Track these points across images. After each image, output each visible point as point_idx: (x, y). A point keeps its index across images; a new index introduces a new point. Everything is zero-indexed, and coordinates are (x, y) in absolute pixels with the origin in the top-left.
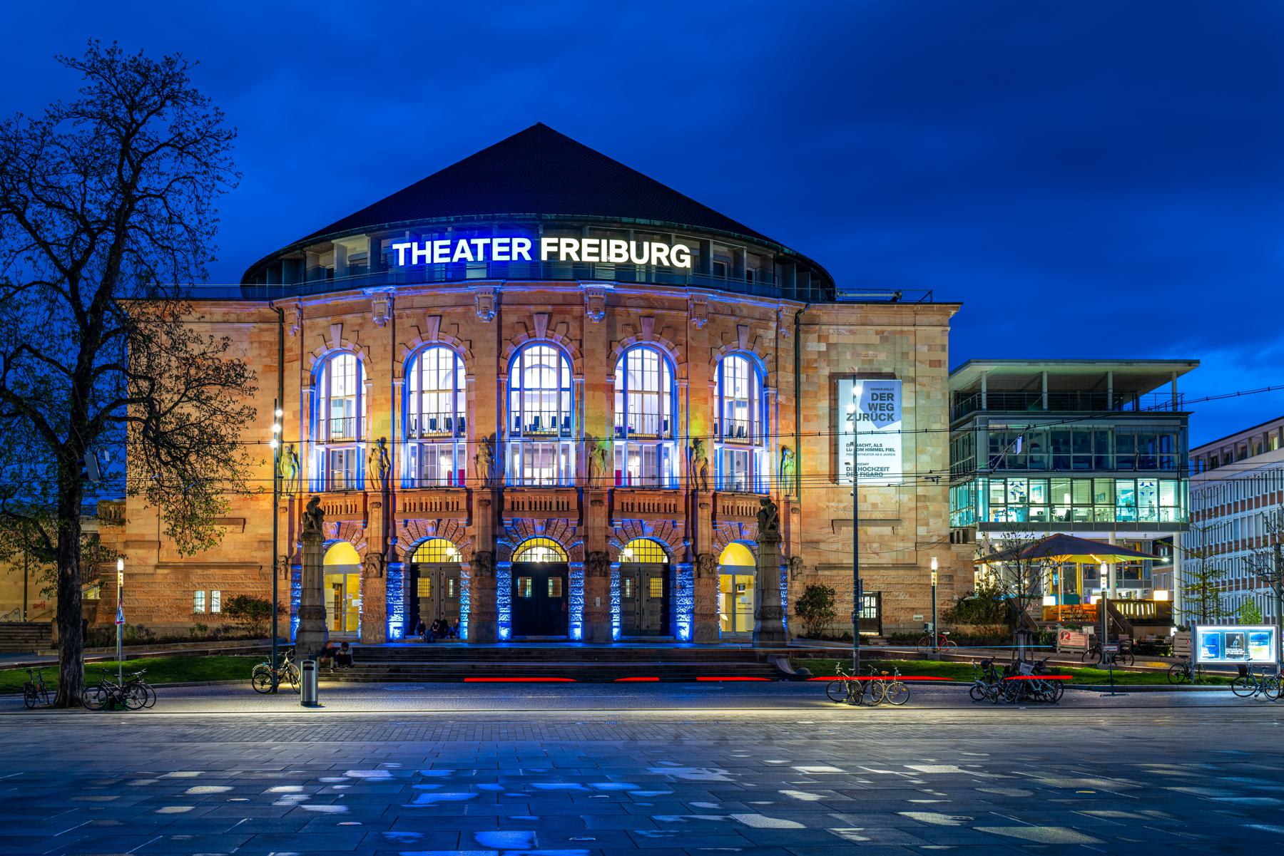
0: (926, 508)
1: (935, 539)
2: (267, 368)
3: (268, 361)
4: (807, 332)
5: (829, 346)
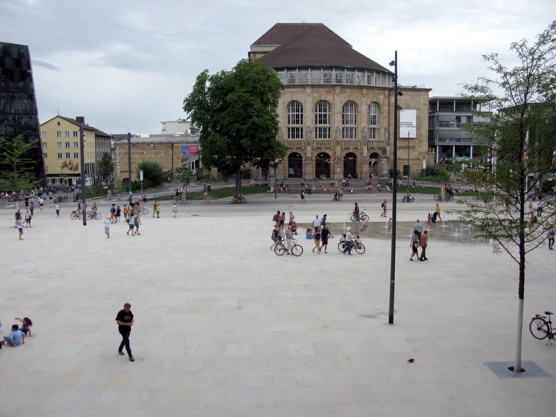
0: (422, 143)
1: (424, 152)
4: (392, 96)
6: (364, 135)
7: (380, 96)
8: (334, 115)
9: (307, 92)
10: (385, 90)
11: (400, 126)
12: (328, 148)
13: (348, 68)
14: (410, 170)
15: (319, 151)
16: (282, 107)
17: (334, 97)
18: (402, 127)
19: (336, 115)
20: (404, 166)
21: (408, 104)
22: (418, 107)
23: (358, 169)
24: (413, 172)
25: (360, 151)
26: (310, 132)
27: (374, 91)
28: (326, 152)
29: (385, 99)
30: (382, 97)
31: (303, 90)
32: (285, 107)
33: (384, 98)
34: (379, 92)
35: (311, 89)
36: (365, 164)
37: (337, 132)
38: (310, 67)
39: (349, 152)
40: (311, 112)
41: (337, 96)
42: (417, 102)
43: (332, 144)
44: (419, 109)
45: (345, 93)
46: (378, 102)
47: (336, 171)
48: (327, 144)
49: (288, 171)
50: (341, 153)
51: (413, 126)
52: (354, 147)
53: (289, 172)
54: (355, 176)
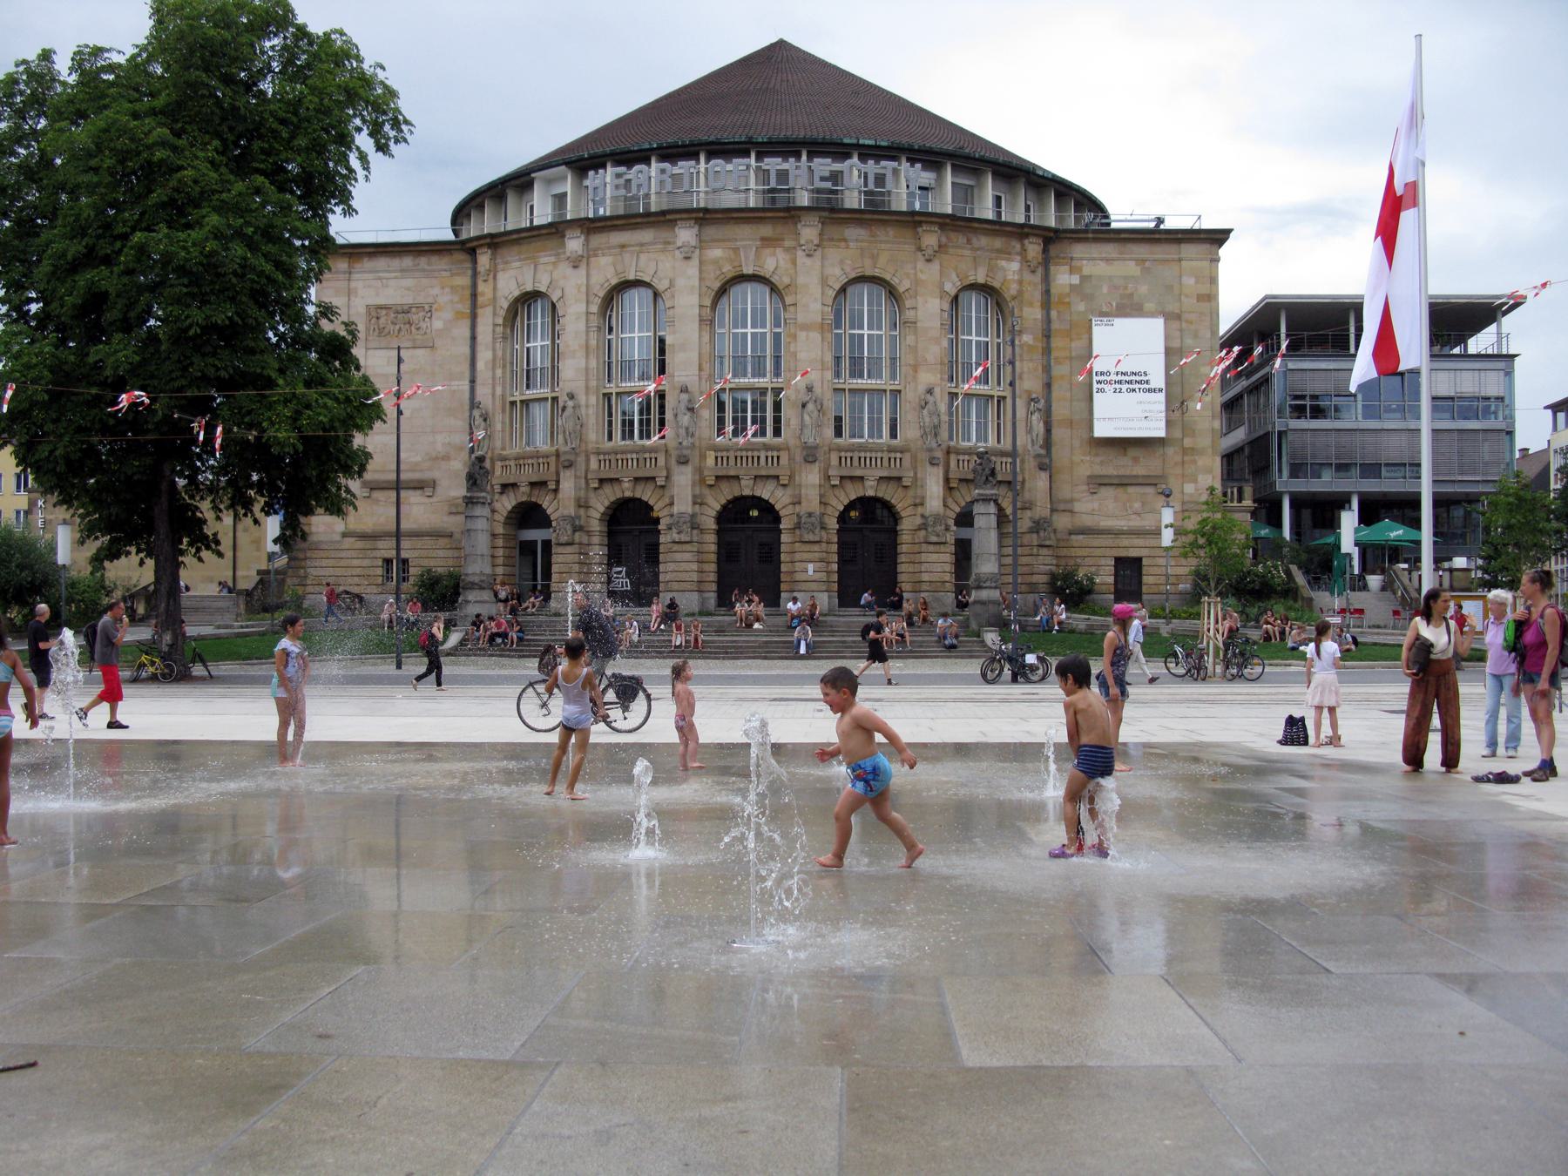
0: (1194, 462)
2: (459, 315)
3: (460, 307)
5: (1084, 279)
6: (927, 420)
7: (1003, 263)
8: (795, 336)
9: (679, 244)
10: (1027, 236)
11: (1095, 386)
12: (768, 477)
13: (864, 146)
14: (1145, 579)
15: (727, 493)
16: (582, 307)
17: (794, 262)
18: (1102, 390)
19: (802, 335)
20: (1118, 560)
21: (1131, 295)
22: (1172, 307)
23: (905, 571)
24: (1155, 589)
25: (911, 493)
26: (691, 410)
27: (974, 240)
28: (757, 493)
29: (1027, 276)
30: (1014, 266)
31: (664, 234)
32: (594, 308)
33: (1021, 270)
34: (998, 243)
35: (695, 230)
36: (931, 548)
37: (804, 406)
38: (701, 144)
39: (861, 494)
40: (696, 325)
41: (809, 255)
42: (1169, 288)
43: (784, 460)
44: (1178, 317)
45: (843, 244)
46: (996, 284)
47: (799, 577)
48: (763, 460)
49: (604, 578)
50: (821, 496)
51: (1152, 386)
52: (885, 474)
53: (609, 581)
54: (890, 598)
